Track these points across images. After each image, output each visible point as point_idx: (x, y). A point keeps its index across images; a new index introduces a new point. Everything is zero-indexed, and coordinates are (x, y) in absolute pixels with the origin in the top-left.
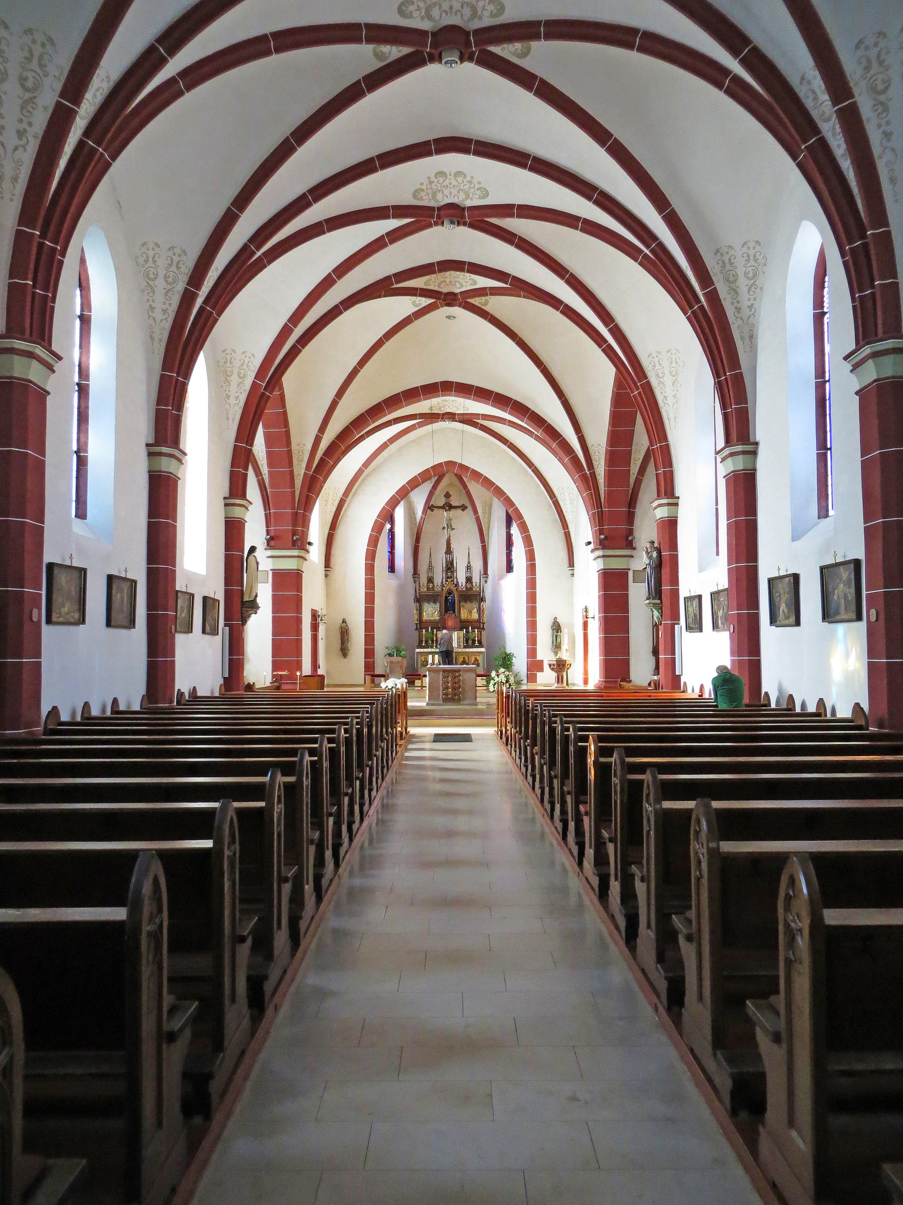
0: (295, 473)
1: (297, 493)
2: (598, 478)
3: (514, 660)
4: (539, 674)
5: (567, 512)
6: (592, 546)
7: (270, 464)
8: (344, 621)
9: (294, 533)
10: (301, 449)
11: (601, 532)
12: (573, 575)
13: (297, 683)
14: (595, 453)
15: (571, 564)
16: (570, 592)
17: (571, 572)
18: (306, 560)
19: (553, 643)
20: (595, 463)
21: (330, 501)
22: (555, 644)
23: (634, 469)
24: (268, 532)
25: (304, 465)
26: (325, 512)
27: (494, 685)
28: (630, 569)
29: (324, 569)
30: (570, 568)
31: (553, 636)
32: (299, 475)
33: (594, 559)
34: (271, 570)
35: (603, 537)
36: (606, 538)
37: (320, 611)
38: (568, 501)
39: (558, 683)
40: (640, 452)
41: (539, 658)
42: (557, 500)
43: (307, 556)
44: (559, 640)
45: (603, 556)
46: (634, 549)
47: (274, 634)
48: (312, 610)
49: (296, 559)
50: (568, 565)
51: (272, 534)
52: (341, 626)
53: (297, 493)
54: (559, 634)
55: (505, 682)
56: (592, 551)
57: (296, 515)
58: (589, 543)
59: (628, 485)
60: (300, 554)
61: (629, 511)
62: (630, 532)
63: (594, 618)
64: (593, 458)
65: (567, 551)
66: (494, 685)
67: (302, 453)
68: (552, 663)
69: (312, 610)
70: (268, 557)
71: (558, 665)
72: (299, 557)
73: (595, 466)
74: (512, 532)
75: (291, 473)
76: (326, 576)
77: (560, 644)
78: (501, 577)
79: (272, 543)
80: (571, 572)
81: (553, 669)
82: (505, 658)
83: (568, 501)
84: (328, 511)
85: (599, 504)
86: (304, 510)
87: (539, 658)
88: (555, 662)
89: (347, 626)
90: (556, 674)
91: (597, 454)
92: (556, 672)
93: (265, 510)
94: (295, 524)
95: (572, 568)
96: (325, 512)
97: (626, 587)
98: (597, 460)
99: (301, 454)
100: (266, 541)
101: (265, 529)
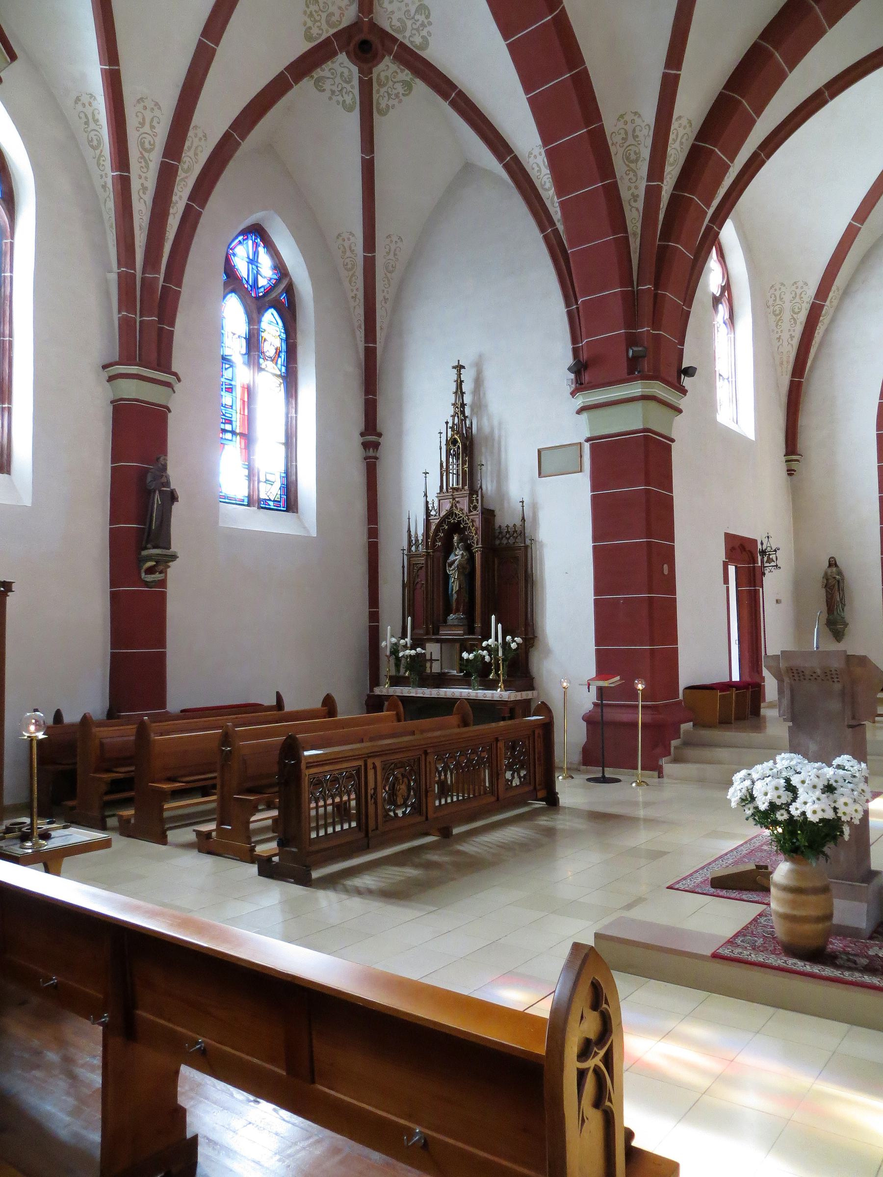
0: (625, 194)
1: (635, 244)
7: (561, 184)
8: (833, 563)
9: (632, 340)
10: (629, 128)
13: (637, 706)
18: (680, 411)
21: (787, 316)
24: (576, 352)
25: (643, 169)
26: (779, 339)
29: (784, 459)
32: (635, 198)
34: (588, 440)
37: (765, 541)
43: (683, 403)
47: (599, 589)
48: (729, 537)
49: (639, 405)
51: (584, 356)
52: (826, 574)
53: (635, 244)
57: (631, 301)
60: (649, 391)
67: (635, 137)
69: (729, 537)
70: (580, 411)
72: (644, 398)
75: (612, 193)
76: (790, 472)
79: (586, 377)
84: (785, 336)
86: (657, 286)
89: (840, 573)
93: (568, 305)
94: (632, 318)
96: (779, 339)
99: (630, 140)
100: (572, 376)
101: (570, 347)
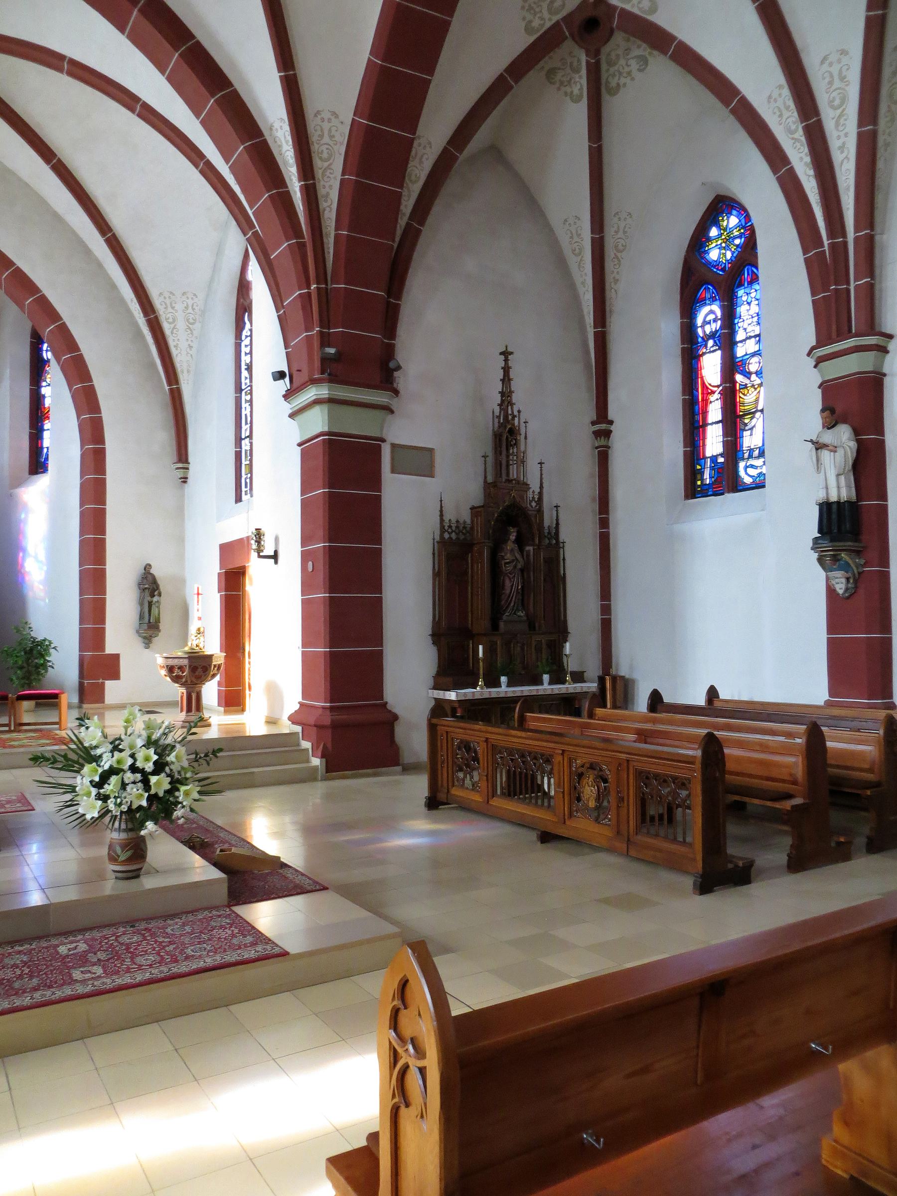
2: (323, 205)
3: (53, 657)
4: (109, 684)
5: (176, 347)
6: (283, 385)
11: (325, 340)
12: (184, 480)
14: (321, 136)
15: (182, 455)
16: (179, 513)
17: (180, 473)
19: (141, 617)
20: (318, 164)
22: (146, 620)
23: (407, 205)
27: (99, 785)
28: (383, 441)
30: (180, 465)
31: (141, 604)
33: (292, 416)
35: (332, 351)
36: (337, 358)
38: (181, 324)
39: (189, 710)
40: (421, 162)
41: (110, 648)
42: (156, 318)
44: (155, 611)
45: (331, 401)
46: (396, 392)
50: (175, 459)
54: (155, 599)
55: (149, 767)
56: (287, 396)
58: (280, 375)
59: (394, 241)
61: (388, 303)
62: (389, 352)
63: (275, 557)
64: (315, 148)
65: (173, 432)
66: (99, 785)
68: (175, 662)
71: (193, 669)
73: (318, 173)
74: (45, 391)
77: (158, 621)
78: (18, 482)
80: (180, 473)
81: (176, 679)
82: (31, 650)
83: (181, 324)
85: (322, 277)
87: (110, 648)
88: (185, 662)
90: (183, 690)
91: (326, 139)
92: (183, 685)
95: (185, 465)
97: (375, 481)
98: (325, 155)
